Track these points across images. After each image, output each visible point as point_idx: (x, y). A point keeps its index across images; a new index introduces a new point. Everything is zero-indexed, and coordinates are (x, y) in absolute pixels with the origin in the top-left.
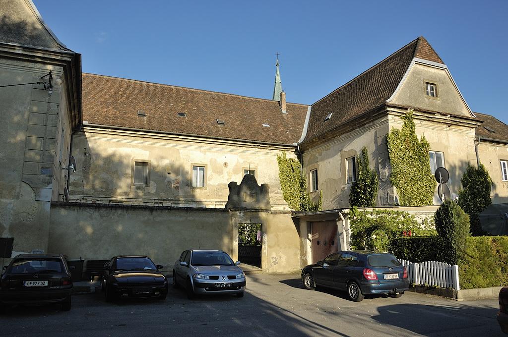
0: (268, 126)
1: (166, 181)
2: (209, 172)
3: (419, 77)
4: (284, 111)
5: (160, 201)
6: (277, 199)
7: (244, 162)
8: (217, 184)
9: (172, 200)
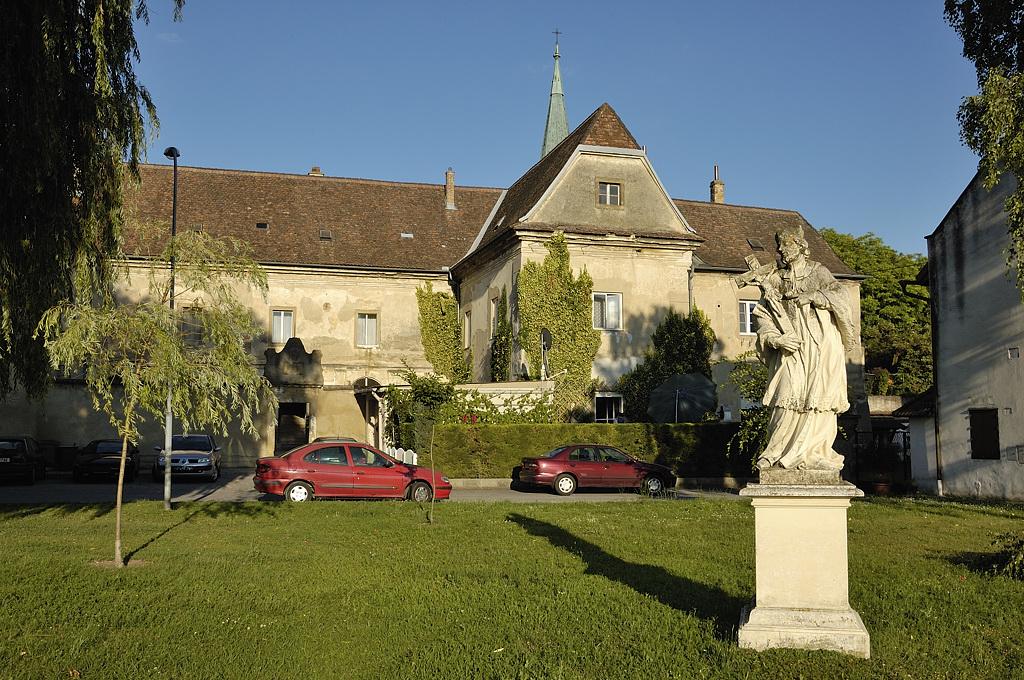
0: (411, 236)
3: (587, 174)
4: (450, 206)
6: (414, 360)
7: (358, 300)
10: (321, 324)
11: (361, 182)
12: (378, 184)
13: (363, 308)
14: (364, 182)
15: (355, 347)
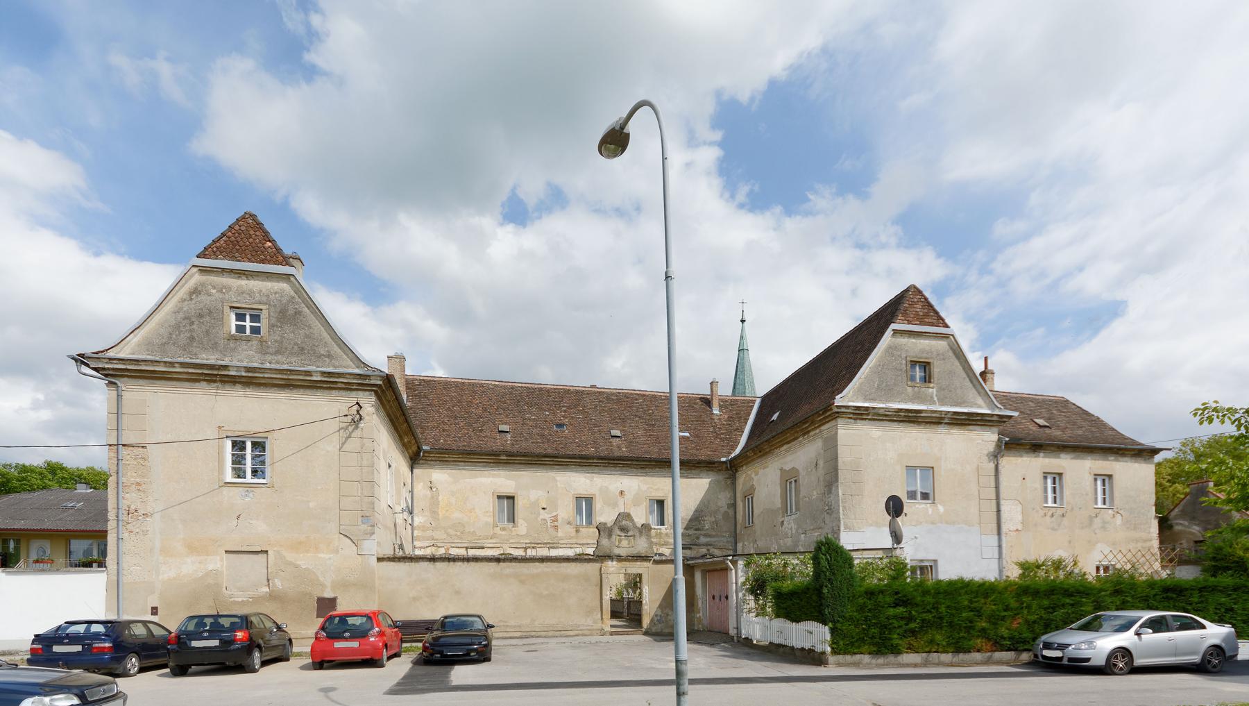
0: (687, 434)
2: (598, 505)
4: (716, 411)
5: (533, 545)
7: (648, 488)
9: (549, 543)
11: (638, 392)
13: (653, 494)
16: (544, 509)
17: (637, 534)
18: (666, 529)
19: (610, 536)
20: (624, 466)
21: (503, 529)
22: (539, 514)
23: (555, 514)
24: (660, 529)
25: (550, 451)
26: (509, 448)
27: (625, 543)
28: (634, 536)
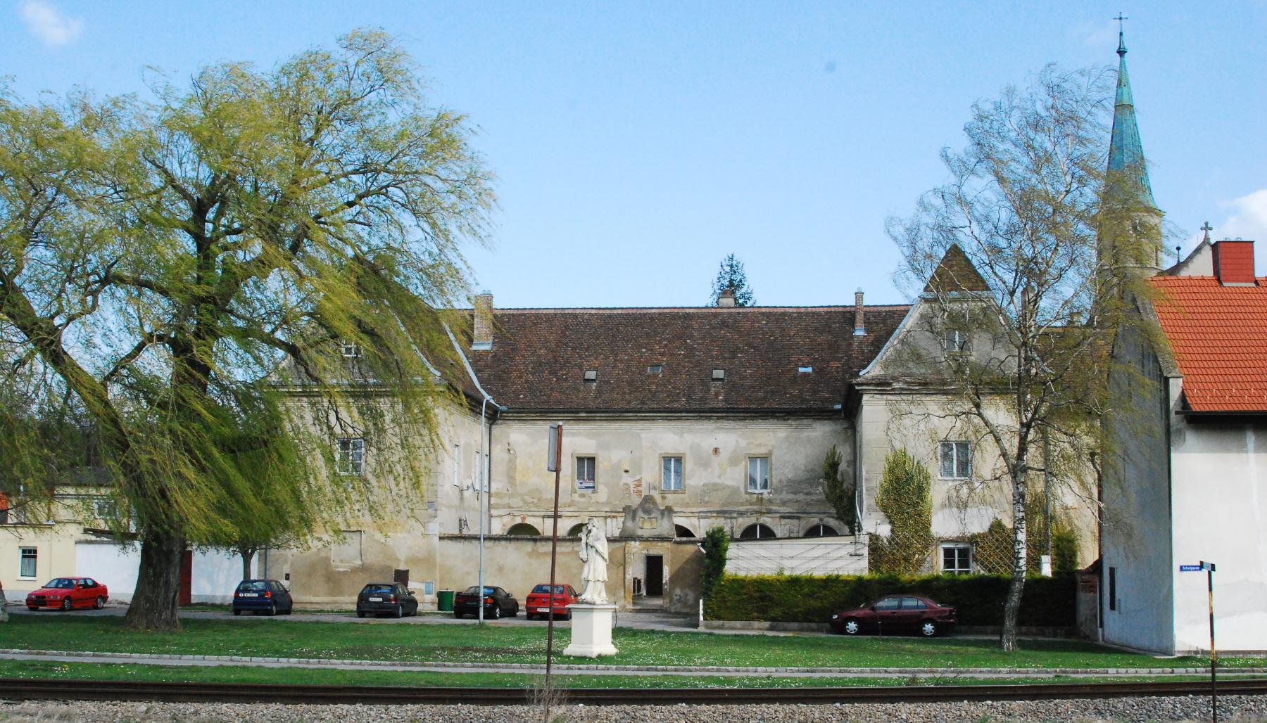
0: (809, 370)
1: (621, 484)
2: (689, 465)
5: (613, 514)
7: (748, 444)
8: (702, 484)
10: (710, 470)
11: (764, 310)
12: (782, 310)
14: (767, 310)
15: (747, 493)
16: (626, 471)
17: (660, 516)
18: (769, 493)
19: (634, 518)
20: (719, 418)
21: (582, 496)
22: (621, 477)
23: (638, 477)
24: (762, 494)
25: (634, 404)
26: (592, 405)
27: (647, 525)
28: (656, 518)
